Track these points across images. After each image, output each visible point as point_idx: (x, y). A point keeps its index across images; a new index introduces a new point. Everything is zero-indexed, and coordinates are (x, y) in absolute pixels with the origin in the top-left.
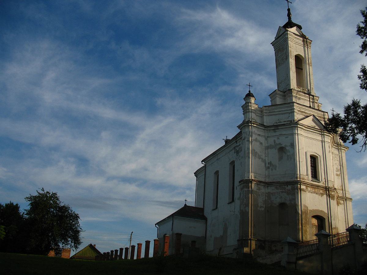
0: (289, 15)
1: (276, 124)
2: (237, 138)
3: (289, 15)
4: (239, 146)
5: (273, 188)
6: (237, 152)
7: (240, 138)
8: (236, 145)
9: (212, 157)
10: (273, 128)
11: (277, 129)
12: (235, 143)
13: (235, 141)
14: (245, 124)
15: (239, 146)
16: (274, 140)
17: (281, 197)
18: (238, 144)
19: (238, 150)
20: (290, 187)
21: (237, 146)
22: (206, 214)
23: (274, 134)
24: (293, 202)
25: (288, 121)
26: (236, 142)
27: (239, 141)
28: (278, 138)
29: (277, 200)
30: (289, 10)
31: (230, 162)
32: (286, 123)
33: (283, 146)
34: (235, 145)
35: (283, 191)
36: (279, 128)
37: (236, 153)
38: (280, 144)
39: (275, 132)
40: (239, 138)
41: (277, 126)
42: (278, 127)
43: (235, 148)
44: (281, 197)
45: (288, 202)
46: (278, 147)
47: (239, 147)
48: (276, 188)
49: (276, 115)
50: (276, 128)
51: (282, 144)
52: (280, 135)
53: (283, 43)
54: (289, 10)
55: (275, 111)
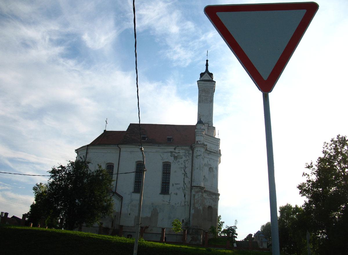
0: (207, 65)
1: (209, 150)
2: (178, 147)
3: (207, 65)
4: (178, 153)
5: (206, 194)
6: (176, 158)
7: (182, 148)
8: (175, 151)
9: (135, 146)
10: (209, 153)
11: (209, 154)
12: (173, 149)
13: (174, 148)
14: (203, 146)
15: (178, 153)
16: (208, 161)
17: (210, 202)
18: (177, 151)
19: (176, 155)
20: (214, 197)
21: (175, 152)
22: (118, 192)
23: (208, 156)
24: (215, 207)
25: (215, 151)
26: (175, 149)
27: (178, 149)
28: (209, 160)
29: (208, 204)
30: (207, 61)
31: (163, 161)
32: (214, 151)
33: (212, 166)
34: (173, 150)
35: (211, 198)
36: (212, 154)
37: (173, 157)
38: (210, 165)
39: (208, 155)
40: (180, 148)
41: (211, 152)
42: (211, 152)
43: (171, 152)
44: (210, 202)
45: (213, 206)
46: (210, 166)
47: (179, 154)
48: (207, 195)
49: (210, 143)
50: (210, 153)
51: (211, 166)
52: (211, 158)
53: (209, 88)
54: (207, 61)
55: (210, 140)
